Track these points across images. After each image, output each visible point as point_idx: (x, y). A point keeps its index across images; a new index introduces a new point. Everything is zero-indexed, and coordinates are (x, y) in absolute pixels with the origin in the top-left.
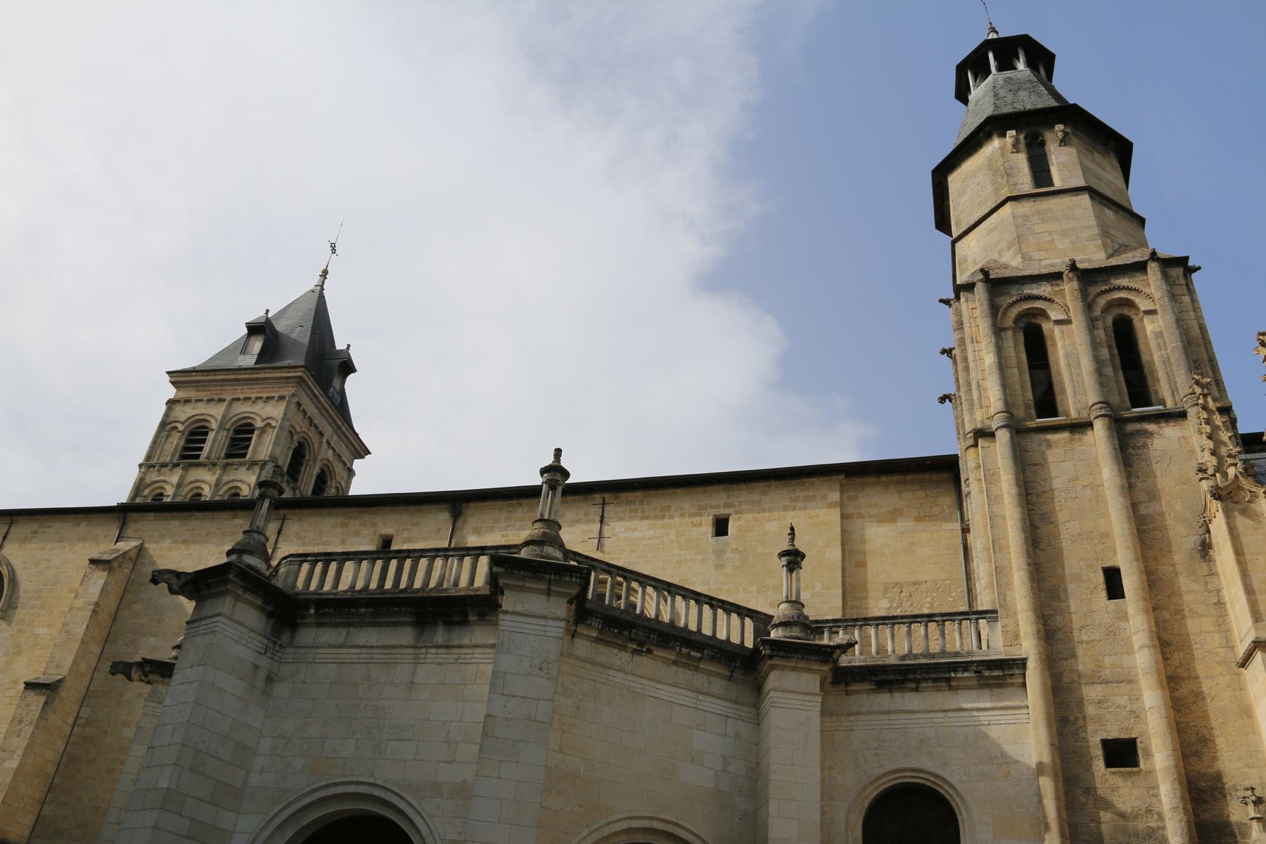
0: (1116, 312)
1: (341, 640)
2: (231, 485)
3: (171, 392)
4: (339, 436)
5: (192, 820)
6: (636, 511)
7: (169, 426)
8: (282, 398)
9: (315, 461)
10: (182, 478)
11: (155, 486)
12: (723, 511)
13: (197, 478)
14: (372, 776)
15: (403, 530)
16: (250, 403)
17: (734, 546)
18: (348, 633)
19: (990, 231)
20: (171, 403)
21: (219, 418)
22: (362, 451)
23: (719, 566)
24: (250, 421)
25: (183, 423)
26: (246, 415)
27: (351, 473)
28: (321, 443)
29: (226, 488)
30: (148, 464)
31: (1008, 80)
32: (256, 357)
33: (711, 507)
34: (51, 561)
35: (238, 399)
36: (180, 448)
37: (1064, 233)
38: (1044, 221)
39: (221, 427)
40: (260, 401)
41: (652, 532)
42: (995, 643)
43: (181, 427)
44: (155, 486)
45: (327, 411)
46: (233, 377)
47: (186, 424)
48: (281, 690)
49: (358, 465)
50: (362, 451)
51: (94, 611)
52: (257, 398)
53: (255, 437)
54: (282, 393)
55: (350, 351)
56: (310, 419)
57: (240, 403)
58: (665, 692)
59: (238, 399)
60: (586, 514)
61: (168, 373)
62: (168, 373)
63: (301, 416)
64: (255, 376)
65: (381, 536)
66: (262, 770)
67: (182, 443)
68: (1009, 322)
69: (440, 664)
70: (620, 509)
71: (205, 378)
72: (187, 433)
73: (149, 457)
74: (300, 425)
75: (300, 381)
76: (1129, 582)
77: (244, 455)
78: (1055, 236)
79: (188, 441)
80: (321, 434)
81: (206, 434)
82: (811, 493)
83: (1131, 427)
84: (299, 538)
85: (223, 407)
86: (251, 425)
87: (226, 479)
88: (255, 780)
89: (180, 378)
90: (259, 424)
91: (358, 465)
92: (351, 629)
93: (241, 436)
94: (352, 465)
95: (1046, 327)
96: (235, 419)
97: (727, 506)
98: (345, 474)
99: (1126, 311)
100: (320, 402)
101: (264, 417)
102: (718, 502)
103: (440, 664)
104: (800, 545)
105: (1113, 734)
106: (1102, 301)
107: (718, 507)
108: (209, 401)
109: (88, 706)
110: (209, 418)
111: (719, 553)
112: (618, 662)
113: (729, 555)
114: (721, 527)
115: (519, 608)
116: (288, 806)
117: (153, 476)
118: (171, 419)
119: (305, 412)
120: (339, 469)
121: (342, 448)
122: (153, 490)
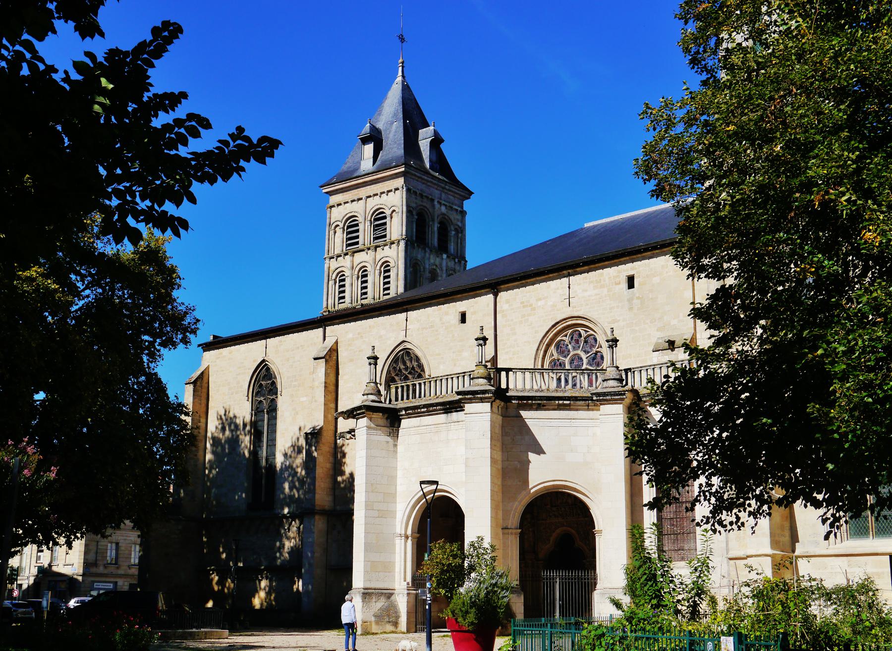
8: (397, 189)
9: (433, 220)
12: (631, 273)
17: (637, 295)
22: (468, 194)
27: (463, 213)
33: (624, 271)
35: (370, 197)
36: (345, 240)
43: (341, 225)
50: (468, 194)
51: (325, 387)
53: (388, 220)
54: (396, 186)
57: (372, 198)
59: (370, 197)
69: (456, 430)
79: (348, 233)
86: (383, 213)
90: (388, 212)
94: (462, 207)
97: (632, 269)
98: (459, 217)
103: (456, 430)
104: (617, 335)
108: (352, 201)
110: (356, 214)
111: (630, 300)
113: (635, 301)
116: (413, 497)
120: (454, 217)
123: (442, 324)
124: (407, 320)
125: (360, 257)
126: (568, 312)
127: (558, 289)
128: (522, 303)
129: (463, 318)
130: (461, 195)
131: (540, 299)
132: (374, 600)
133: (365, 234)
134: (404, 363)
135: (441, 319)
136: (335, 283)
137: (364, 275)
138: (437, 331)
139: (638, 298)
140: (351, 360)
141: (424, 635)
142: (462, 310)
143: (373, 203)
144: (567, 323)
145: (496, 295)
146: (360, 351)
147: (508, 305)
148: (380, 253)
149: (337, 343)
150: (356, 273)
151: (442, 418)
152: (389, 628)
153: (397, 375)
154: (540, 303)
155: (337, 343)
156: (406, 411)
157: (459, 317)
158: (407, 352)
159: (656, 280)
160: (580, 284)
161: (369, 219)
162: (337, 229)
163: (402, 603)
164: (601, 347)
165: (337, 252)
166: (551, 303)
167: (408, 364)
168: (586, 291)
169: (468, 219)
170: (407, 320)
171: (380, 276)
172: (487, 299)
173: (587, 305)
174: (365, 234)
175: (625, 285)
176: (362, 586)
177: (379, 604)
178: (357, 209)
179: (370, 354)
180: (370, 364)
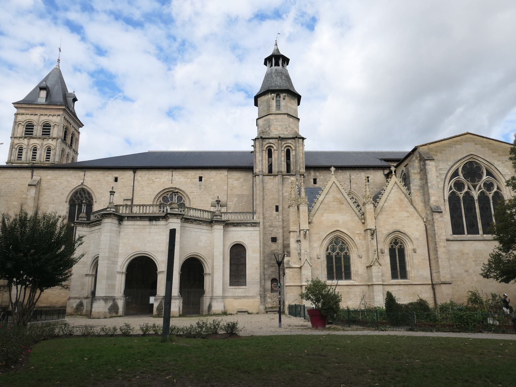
0: (287, 148)
1: (133, 224)
2: (47, 145)
3: (15, 111)
4: (75, 123)
5: (112, 261)
6: (180, 174)
7: (18, 123)
8: (59, 115)
10: (28, 142)
12: (201, 175)
13: (34, 143)
16: (47, 116)
19: (265, 120)
20: (16, 114)
21: (37, 121)
23: (200, 189)
25: (23, 122)
26: (46, 121)
27: (79, 133)
28: (71, 127)
29: (46, 146)
30: (13, 137)
31: (276, 70)
32: (45, 99)
34: (10, 182)
36: (24, 131)
37: (280, 126)
38: (276, 122)
40: (51, 116)
41: (185, 180)
42: (256, 219)
43: (23, 124)
45: (72, 117)
47: (24, 123)
48: (122, 234)
49: (80, 130)
50: (81, 125)
53: (51, 128)
55: (75, 93)
56: (68, 121)
57: (43, 116)
58: (196, 230)
60: (168, 174)
61: (13, 103)
62: (13, 103)
63: (65, 120)
66: (121, 250)
67: (24, 129)
68: (265, 149)
70: (176, 173)
71: (28, 106)
72: (25, 126)
73: (13, 134)
74: (66, 124)
75: (64, 110)
76: (280, 209)
78: (278, 126)
80: (71, 124)
83: (285, 177)
84: (91, 177)
85: (36, 117)
87: (45, 143)
88: (120, 251)
89: (18, 105)
90: (52, 124)
91: (80, 130)
93: (47, 128)
95: (273, 150)
96: (43, 122)
97: (202, 174)
98: (78, 134)
99: (289, 148)
100: (70, 114)
101: (54, 122)
102: (200, 173)
105: (273, 236)
106: (285, 146)
107: (200, 174)
112: (187, 226)
113: (202, 186)
114: (201, 179)
115: (172, 222)
117: (16, 141)
118: (17, 121)
119: (66, 119)
121: (76, 126)
125: (33, 141)
126: (171, 186)
128: (149, 178)
129: (116, 180)
130: (80, 125)
131: (157, 178)
132: (109, 302)
133: (38, 131)
134: (80, 194)
135: (104, 178)
136: (31, 150)
137: (35, 150)
138: (101, 183)
139: (204, 185)
140: (49, 189)
141: (278, 315)
142: (116, 176)
143: (44, 118)
144: (170, 190)
145: (135, 172)
146: (54, 185)
147: (140, 178)
148: (45, 142)
149: (41, 179)
150: (30, 147)
151: (147, 223)
152: (114, 315)
153: (76, 199)
154: (157, 180)
155: (41, 179)
157: (114, 179)
158: (83, 190)
159: (212, 180)
160: (177, 176)
161: (41, 124)
162: (20, 125)
163: (121, 304)
164: (184, 201)
165: (18, 136)
166: (163, 181)
167: (84, 195)
168: (180, 179)
169: (80, 135)
171: (45, 151)
172: (130, 173)
173: (180, 184)
174: (38, 131)
175: (198, 180)
176: (104, 296)
177: (110, 304)
178: (34, 119)
179: (111, 190)
180: (111, 195)
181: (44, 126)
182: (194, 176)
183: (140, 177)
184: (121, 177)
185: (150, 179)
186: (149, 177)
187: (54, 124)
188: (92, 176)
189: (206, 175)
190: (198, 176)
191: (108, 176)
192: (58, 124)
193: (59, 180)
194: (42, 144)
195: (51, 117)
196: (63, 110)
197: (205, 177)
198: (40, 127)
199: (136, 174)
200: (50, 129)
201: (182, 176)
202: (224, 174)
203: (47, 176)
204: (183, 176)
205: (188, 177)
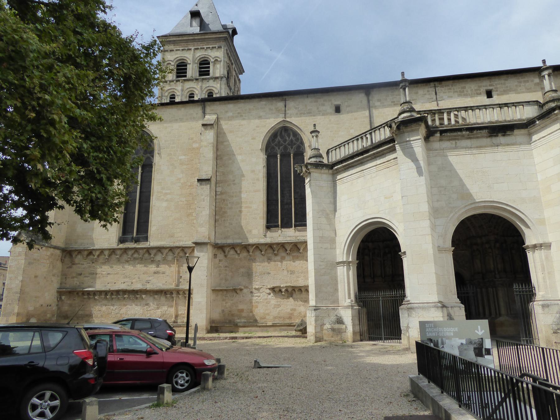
2: (208, 88)
6: (450, 89)
11: (170, 91)
12: (490, 88)
14: (491, 198)
15: (345, 102)
16: (204, 50)
18: (456, 143)
24: (206, 59)
26: (203, 56)
29: (206, 90)
33: (484, 86)
39: (194, 62)
40: (209, 49)
44: (170, 91)
46: (192, 38)
47: (175, 61)
49: (240, 76)
52: (212, 48)
53: (211, 65)
57: (198, 50)
59: (198, 49)
60: (428, 91)
64: (203, 37)
65: (335, 105)
71: (178, 39)
77: (208, 74)
81: (186, 66)
82: (526, 79)
84: (296, 108)
86: (207, 60)
87: (204, 86)
92: (457, 141)
97: (490, 85)
101: (213, 57)
102: (486, 84)
107: (486, 86)
108: (182, 50)
109: (219, 187)
122: (169, 93)
123: (319, 111)
124: (285, 107)
125: (188, 85)
127: (425, 94)
128: (394, 102)
133: (192, 70)
134: (282, 137)
135: (318, 108)
143: (200, 54)
156: (441, 134)
160: (445, 93)
161: (197, 62)
169: (242, 84)
170: (285, 107)
174: (192, 70)
181: (200, 64)
182: (476, 90)
183: (379, 100)
184: (346, 104)
185: (396, 103)
186: (394, 100)
187: (215, 59)
188: (297, 107)
189: (498, 86)
190: (483, 90)
191: (323, 105)
192: (219, 60)
193: (245, 116)
194: (201, 87)
195: (209, 51)
196: (225, 40)
197: (497, 91)
198: (196, 65)
199: (370, 98)
200: (209, 67)
201: (454, 92)
202: (533, 81)
203: (227, 112)
204: (456, 92)
205: (465, 93)
